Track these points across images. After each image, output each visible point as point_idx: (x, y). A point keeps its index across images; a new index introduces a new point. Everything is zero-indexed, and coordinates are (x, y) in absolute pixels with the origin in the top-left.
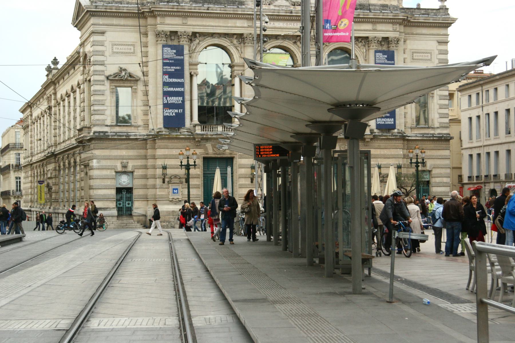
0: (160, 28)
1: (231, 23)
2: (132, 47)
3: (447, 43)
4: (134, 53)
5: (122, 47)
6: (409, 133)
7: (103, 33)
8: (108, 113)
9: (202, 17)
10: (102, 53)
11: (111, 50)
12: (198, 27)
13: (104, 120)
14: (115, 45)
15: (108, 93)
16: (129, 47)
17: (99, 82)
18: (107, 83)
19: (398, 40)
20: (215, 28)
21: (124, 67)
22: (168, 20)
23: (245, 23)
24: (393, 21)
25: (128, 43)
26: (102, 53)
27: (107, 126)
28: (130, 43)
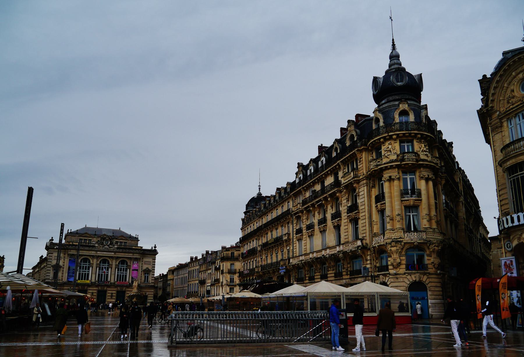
0: (69, 253)
1: (90, 252)
3: (155, 259)
6: (142, 284)
7: (52, 253)
10: (51, 259)
17: (50, 267)
19: (140, 259)
23: (95, 252)
24: (139, 253)
26: (51, 259)
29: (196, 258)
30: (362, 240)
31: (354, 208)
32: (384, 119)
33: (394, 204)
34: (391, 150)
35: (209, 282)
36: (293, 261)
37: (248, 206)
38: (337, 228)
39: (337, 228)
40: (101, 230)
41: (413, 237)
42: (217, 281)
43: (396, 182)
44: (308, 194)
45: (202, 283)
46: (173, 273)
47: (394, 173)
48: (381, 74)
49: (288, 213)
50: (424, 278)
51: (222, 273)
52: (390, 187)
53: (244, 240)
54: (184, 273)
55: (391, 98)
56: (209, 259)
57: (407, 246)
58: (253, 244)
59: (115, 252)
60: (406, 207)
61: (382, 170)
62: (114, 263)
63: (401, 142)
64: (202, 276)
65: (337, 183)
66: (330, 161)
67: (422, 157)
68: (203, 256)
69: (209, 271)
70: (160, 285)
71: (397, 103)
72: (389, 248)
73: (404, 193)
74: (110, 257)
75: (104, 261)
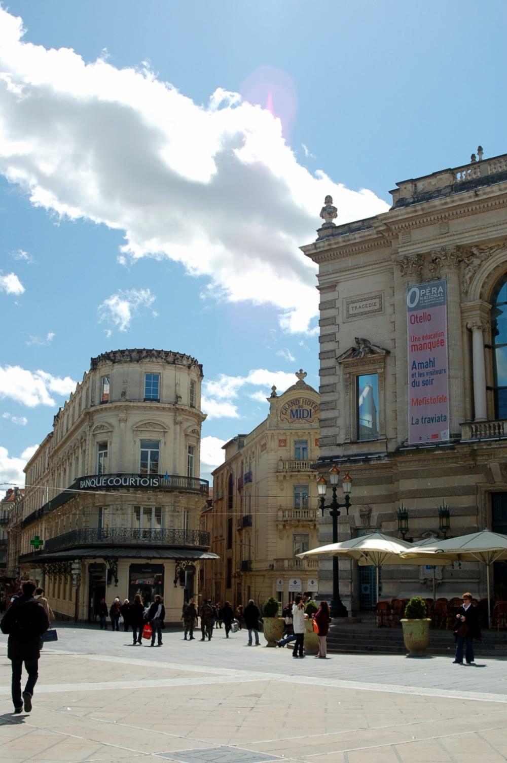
2: (377, 301)
4: (380, 309)
5: (361, 304)
8: (340, 422)
9: (474, 213)
11: (345, 313)
12: (467, 235)
13: (335, 436)
14: (352, 302)
15: (340, 387)
16: (372, 301)
18: (339, 371)
20: (499, 227)
21: (361, 335)
22: (416, 235)
25: (370, 296)
27: (339, 445)
28: (373, 295)
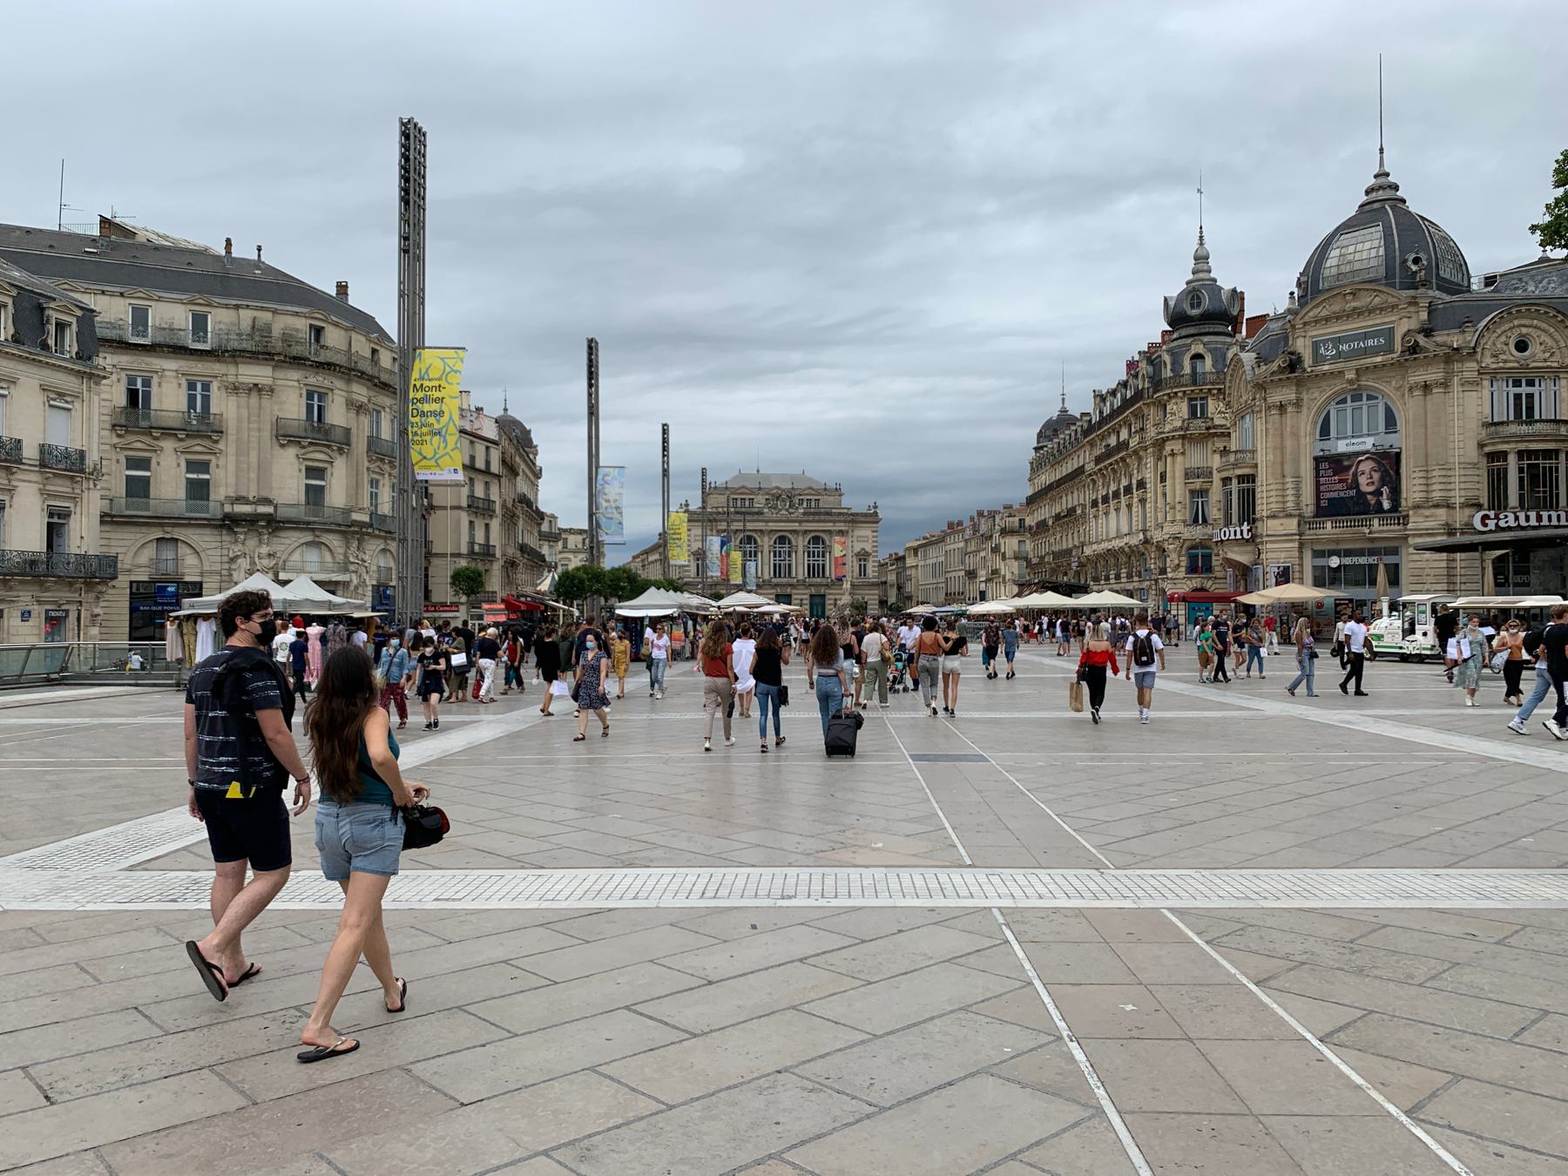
29: (960, 523)
30: (1144, 531)
31: (1141, 484)
32: (1173, 364)
33: (1177, 489)
34: (1179, 410)
35: (982, 574)
36: (1088, 551)
37: (1040, 435)
38: (1129, 506)
39: (1129, 506)
40: (768, 477)
41: (1198, 532)
42: (995, 572)
43: (1179, 459)
44: (1099, 450)
45: (972, 574)
46: (916, 554)
47: (1176, 446)
48: (1175, 288)
49: (1080, 471)
50: (1208, 584)
51: (1004, 558)
52: (1173, 463)
53: (1032, 500)
54: (935, 556)
55: (1184, 332)
56: (983, 528)
57: (1187, 544)
58: (1045, 512)
59: (800, 522)
60: (1192, 492)
61: (1164, 440)
62: (801, 543)
63: (1190, 400)
64: (971, 562)
65: (1125, 445)
66: (1127, 404)
67: (1217, 422)
68: (972, 519)
69: (983, 554)
70: (892, 578)
71: (1189, 341)
72: (1166, 546)
73: (1189, 474)
74: (791, 532)
75: (782, 540)
